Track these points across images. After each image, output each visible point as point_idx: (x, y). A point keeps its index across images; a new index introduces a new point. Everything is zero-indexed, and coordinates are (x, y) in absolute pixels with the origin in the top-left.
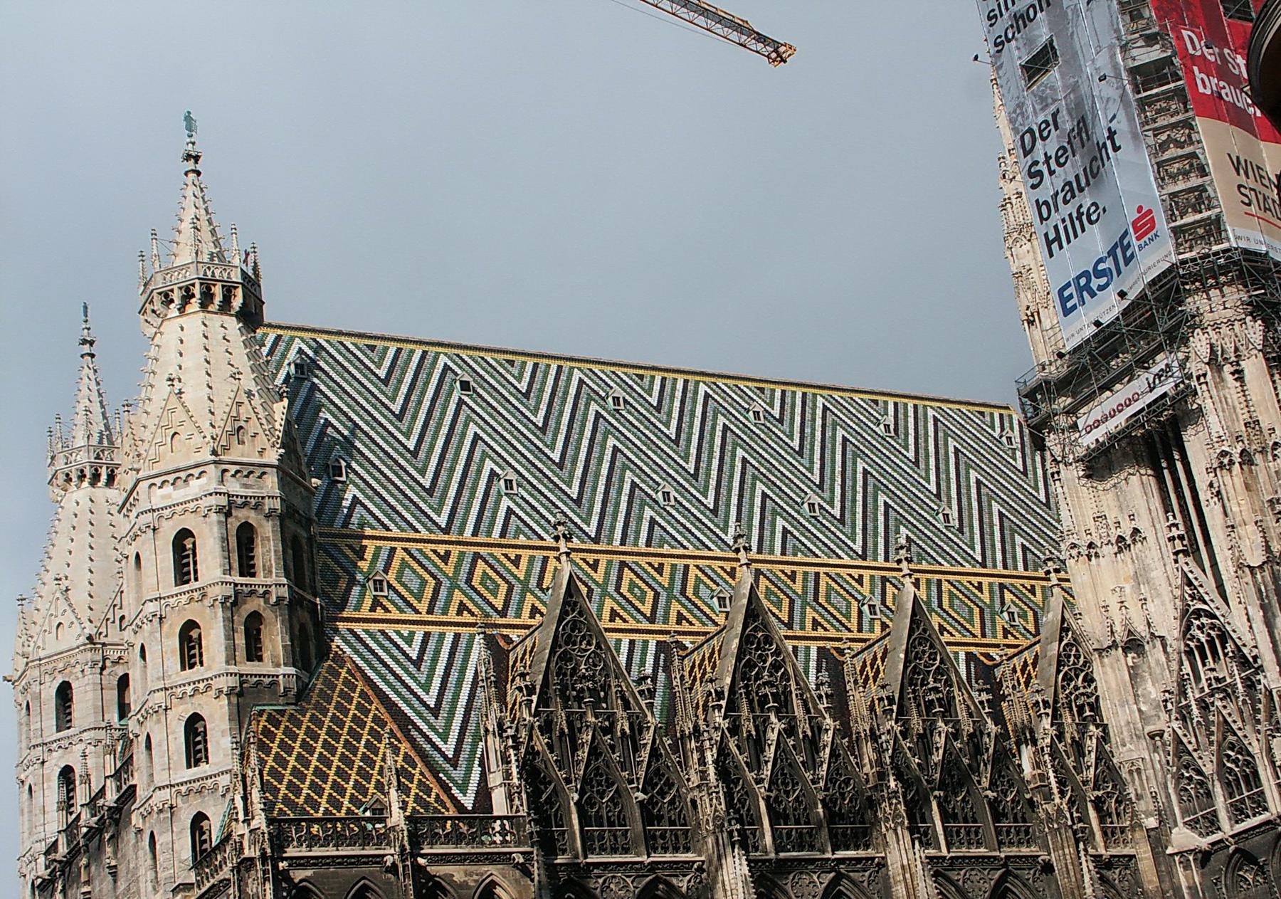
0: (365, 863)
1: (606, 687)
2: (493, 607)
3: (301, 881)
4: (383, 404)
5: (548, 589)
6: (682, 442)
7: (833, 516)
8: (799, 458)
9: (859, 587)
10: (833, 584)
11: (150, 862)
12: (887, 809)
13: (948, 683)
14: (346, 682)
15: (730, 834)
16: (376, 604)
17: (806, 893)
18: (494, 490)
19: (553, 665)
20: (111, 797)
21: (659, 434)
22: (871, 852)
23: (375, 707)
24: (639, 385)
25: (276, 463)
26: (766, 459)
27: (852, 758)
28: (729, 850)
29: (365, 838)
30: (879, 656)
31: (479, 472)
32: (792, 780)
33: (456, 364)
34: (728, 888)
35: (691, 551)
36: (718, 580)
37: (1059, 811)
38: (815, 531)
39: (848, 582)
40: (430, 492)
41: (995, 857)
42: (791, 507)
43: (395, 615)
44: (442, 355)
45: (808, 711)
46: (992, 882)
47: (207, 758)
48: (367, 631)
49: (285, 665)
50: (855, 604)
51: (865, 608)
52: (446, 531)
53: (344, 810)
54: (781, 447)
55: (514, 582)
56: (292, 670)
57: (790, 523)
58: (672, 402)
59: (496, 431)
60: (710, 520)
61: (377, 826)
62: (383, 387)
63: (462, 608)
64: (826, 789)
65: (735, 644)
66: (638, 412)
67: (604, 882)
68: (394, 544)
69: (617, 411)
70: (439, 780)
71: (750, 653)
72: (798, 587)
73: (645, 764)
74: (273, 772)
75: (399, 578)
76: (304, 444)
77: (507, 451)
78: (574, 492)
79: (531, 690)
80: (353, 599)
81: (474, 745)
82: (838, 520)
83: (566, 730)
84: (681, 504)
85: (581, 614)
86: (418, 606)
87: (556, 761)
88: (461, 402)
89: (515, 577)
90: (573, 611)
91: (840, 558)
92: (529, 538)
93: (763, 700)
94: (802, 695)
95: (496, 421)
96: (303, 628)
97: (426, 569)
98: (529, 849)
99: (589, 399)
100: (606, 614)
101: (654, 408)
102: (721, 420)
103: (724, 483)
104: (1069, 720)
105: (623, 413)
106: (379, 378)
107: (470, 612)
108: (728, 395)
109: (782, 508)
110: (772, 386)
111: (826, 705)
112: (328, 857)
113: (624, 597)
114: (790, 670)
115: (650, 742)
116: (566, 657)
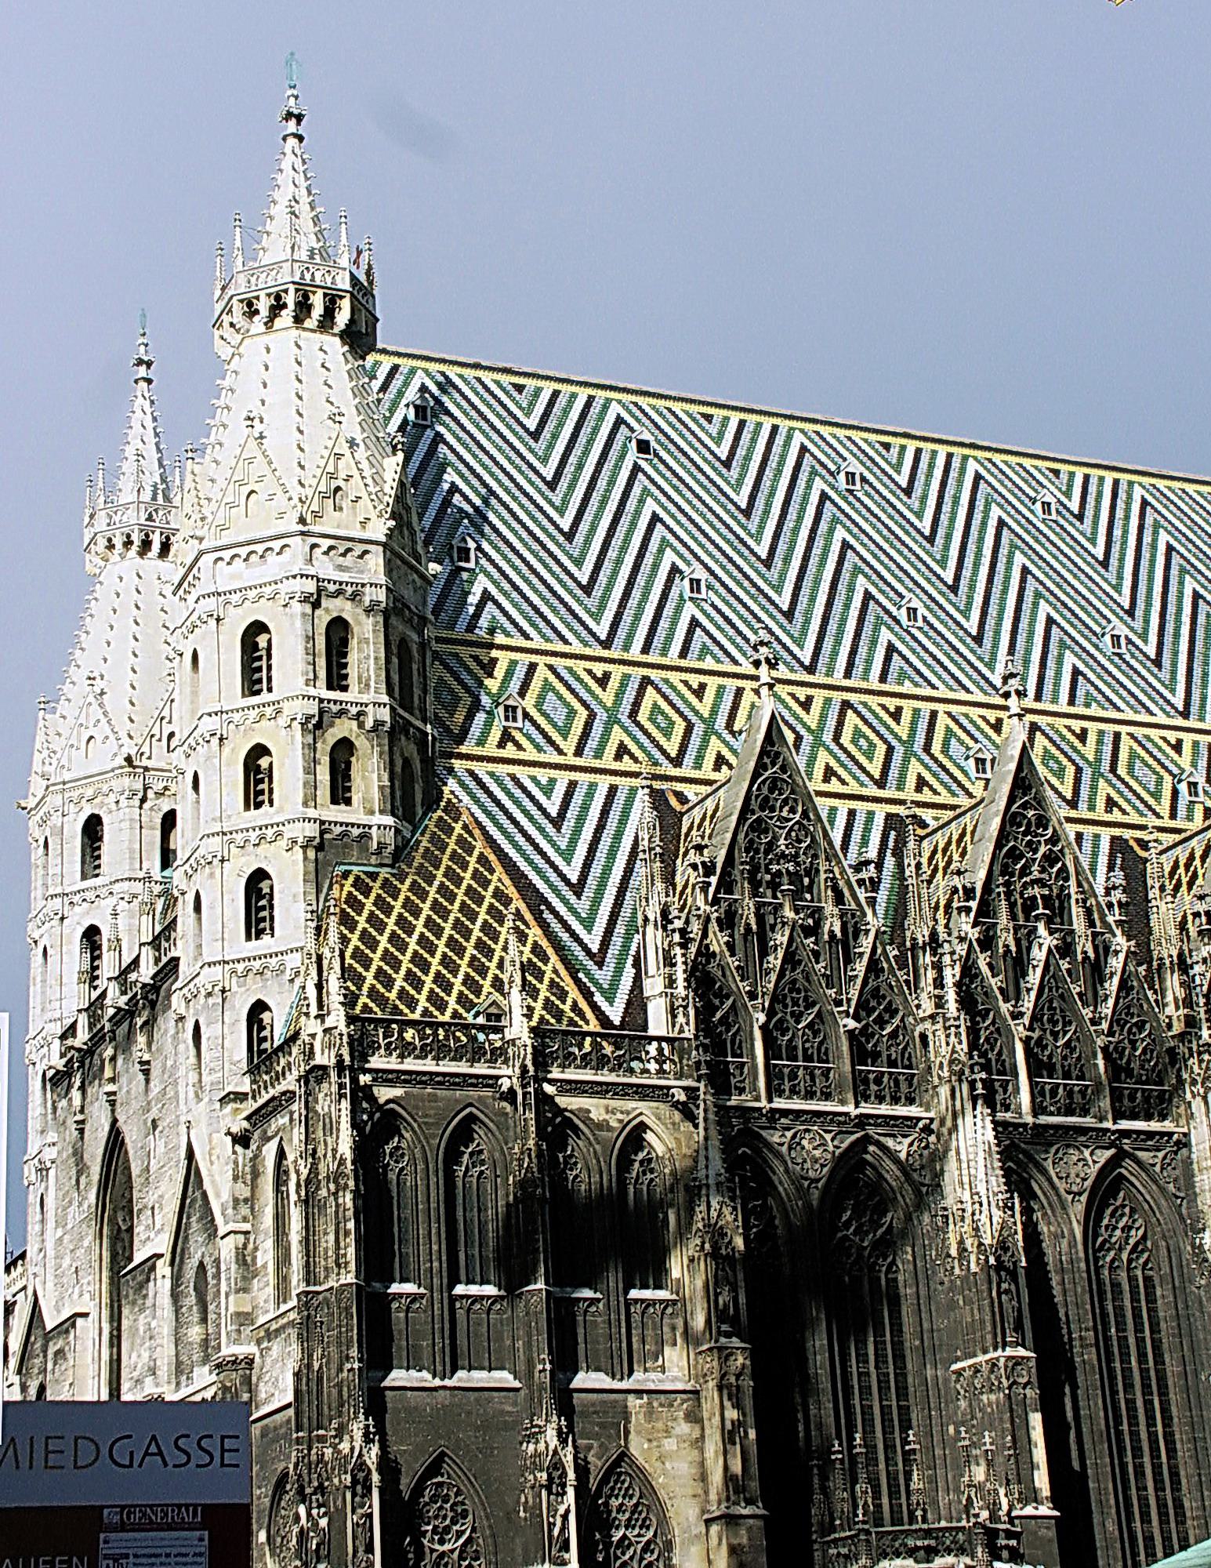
0: (472, 1085)
1: (812, 872)
2: (664, 752)
3: (389, 1101)
4: (530, 466)
5: (741, 732)
6: (939, 540)
7: (1145, 655)
8: (1103, 571)
9: (1175, 757)
10: (1139, 750)
11: (193, 1060)
12: (1196, 1069)
14: (460, 841)
15: (972, 1084)
16: (506, 738)
17: (1073, 1175)
18: (674, 593)
19: (741, 836)
20: (146, 972)
21: (907, 527)
22: (1167, 1125)
23: (499, 877)
24: (883, 457)
25: (383, 539)
26: (1055, 571)
27: (1149, 993)
28: (968, 1106)
29: (476, 1053)
30: (1198, 855)
31: (656, 567)
32: (1064, 1017)
33: (633, 416)
34: (963, 1157)
35: (943, 692)
36: (977, 734)
38: (1119, 675)
39: (1160, 749)
40: (588, 589)
42: (1086, 638)
43: (531, 754)
44: (614, 403)
45: (1091, 924)
47: (272, 929)
48: (492, 774)
49: (382, 812)
50: (1168, 778)
51: (1183, 788)
52: (606, 644)
53: (449, 1012)
54: (1078, 554)
55: (694, 719)
56: (389, 820)
57: (1084, 662)
58: (927, 484)
59: (682, 511)
60: (973, 651)
61: (491, 1036)
62: (531, 442)
63: (622, 751)
64: (1111, 1033)
65: (996, 823)
66: (880, 495)
67: (794, 1136)
68: (534, 658)
69: (851, 492)
70: (578, 982)
71: (1016, 839)
72: (1089, 751)
73: (859, 981)
74: (357, 954)
75: (538, 705)
76: (421, 516)
77: (696, 540)
78: (784, 602)
79: (709, 870)
80: (475, 730)
81: (628, 938)
82: (1153, 661)
83: (754, 927)
84: (931, 626)
85: (783, 769)
87: (738, 968)
88: (636, 469)
89: (696, 713)
90: (773, 764)
91: (1152, 714)
93: (1030, 905)
94: (1084, 901)
95: (683, 496)
98: (695, 1084)
99: (814, 473)
100: (819, 772)
101: (903, 490)
102: (996, 512)
105: (859, 495)
106: (527, 430)
107: (633, 757)
108: (1007, 477)
109: (1073, 639)
110: (1072, 468)
111: (1118, 918)
112: (424, 1073)
113: (845, 750)
115: (869, 951)
116: (759, 827)
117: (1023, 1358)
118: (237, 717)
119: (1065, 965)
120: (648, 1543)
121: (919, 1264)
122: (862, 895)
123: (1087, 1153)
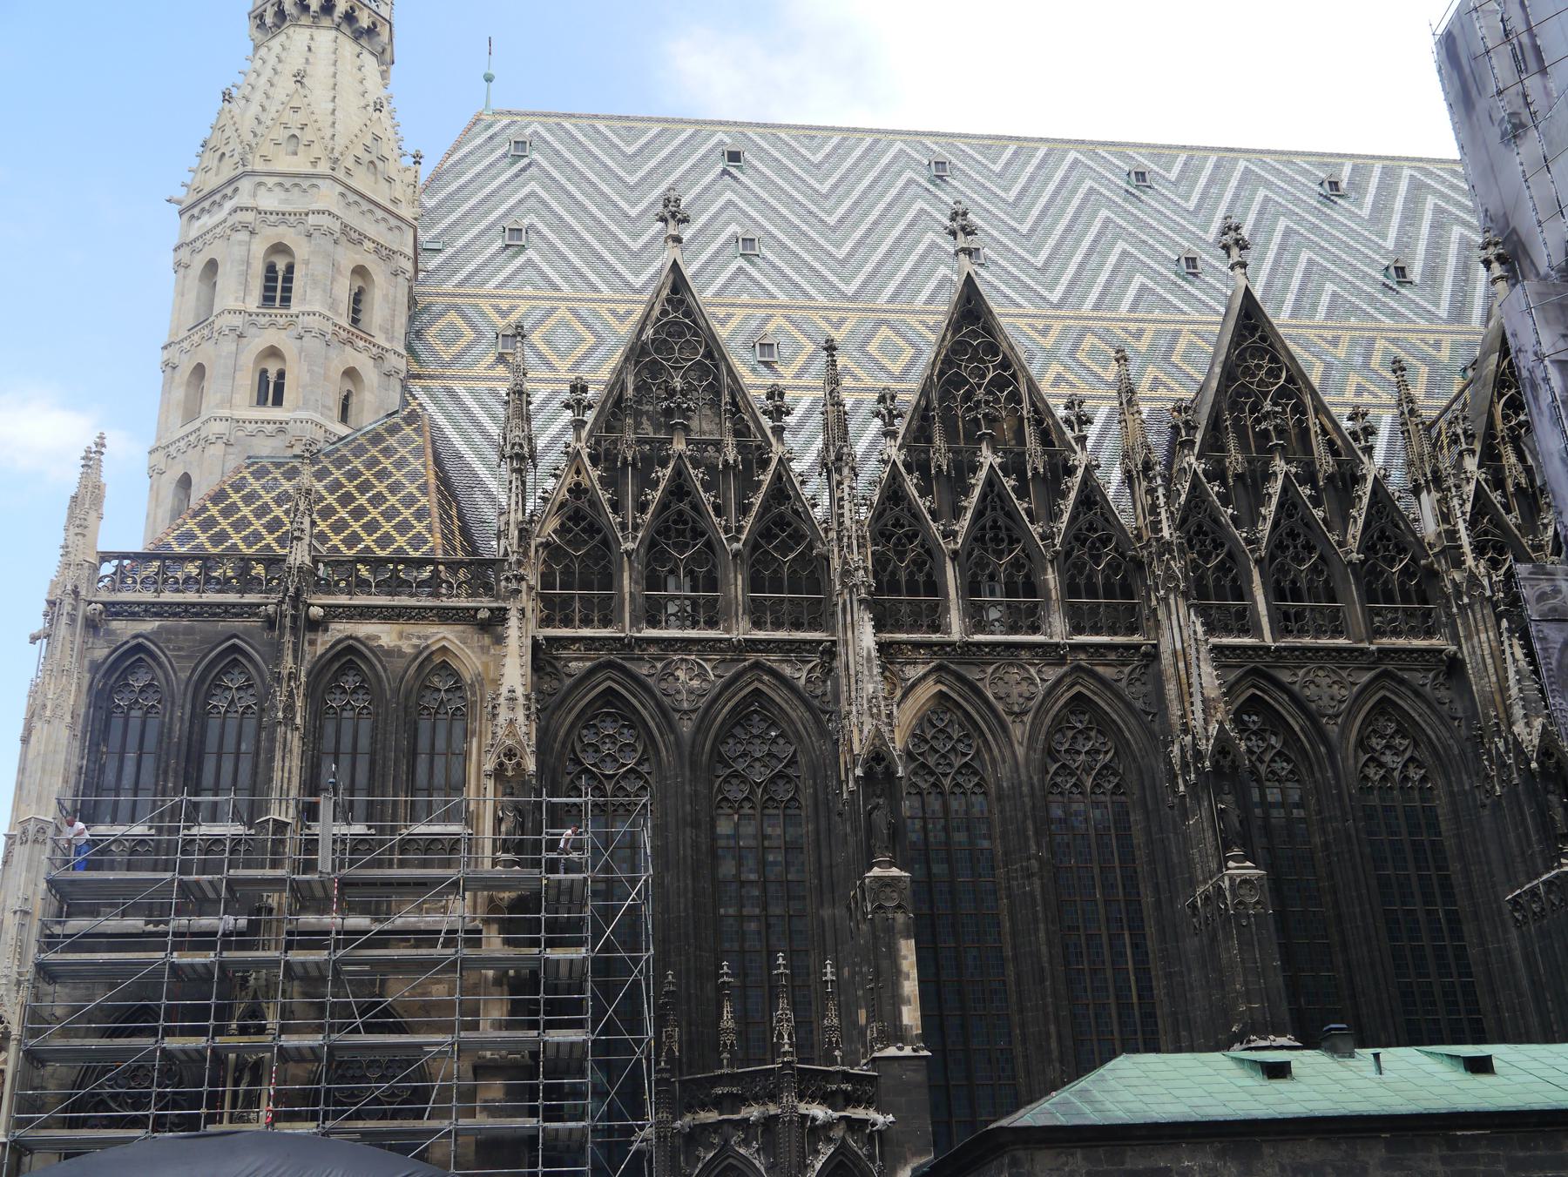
0: (236, 615)
3: (136, 636)
13: (1299, 409)
32: (1010, 537)
34: (852, 672)
37: (1473, 579)
41: (1363, 651)
46: (1355, 689)
67: (664, 668)
68: (555, 304)
71: (959, 366)
73: (755, 509)
80: (468, 359)
87: (609, 500)
92: (752, 296)
96: (351, 373)
104: (1513, 460)
114: (1023, 389)
117: (893, 878)
118: (186, 345)
119: (1009, 483)
121: (821, 796)
122: (767, 423)
123: (1033, 671)
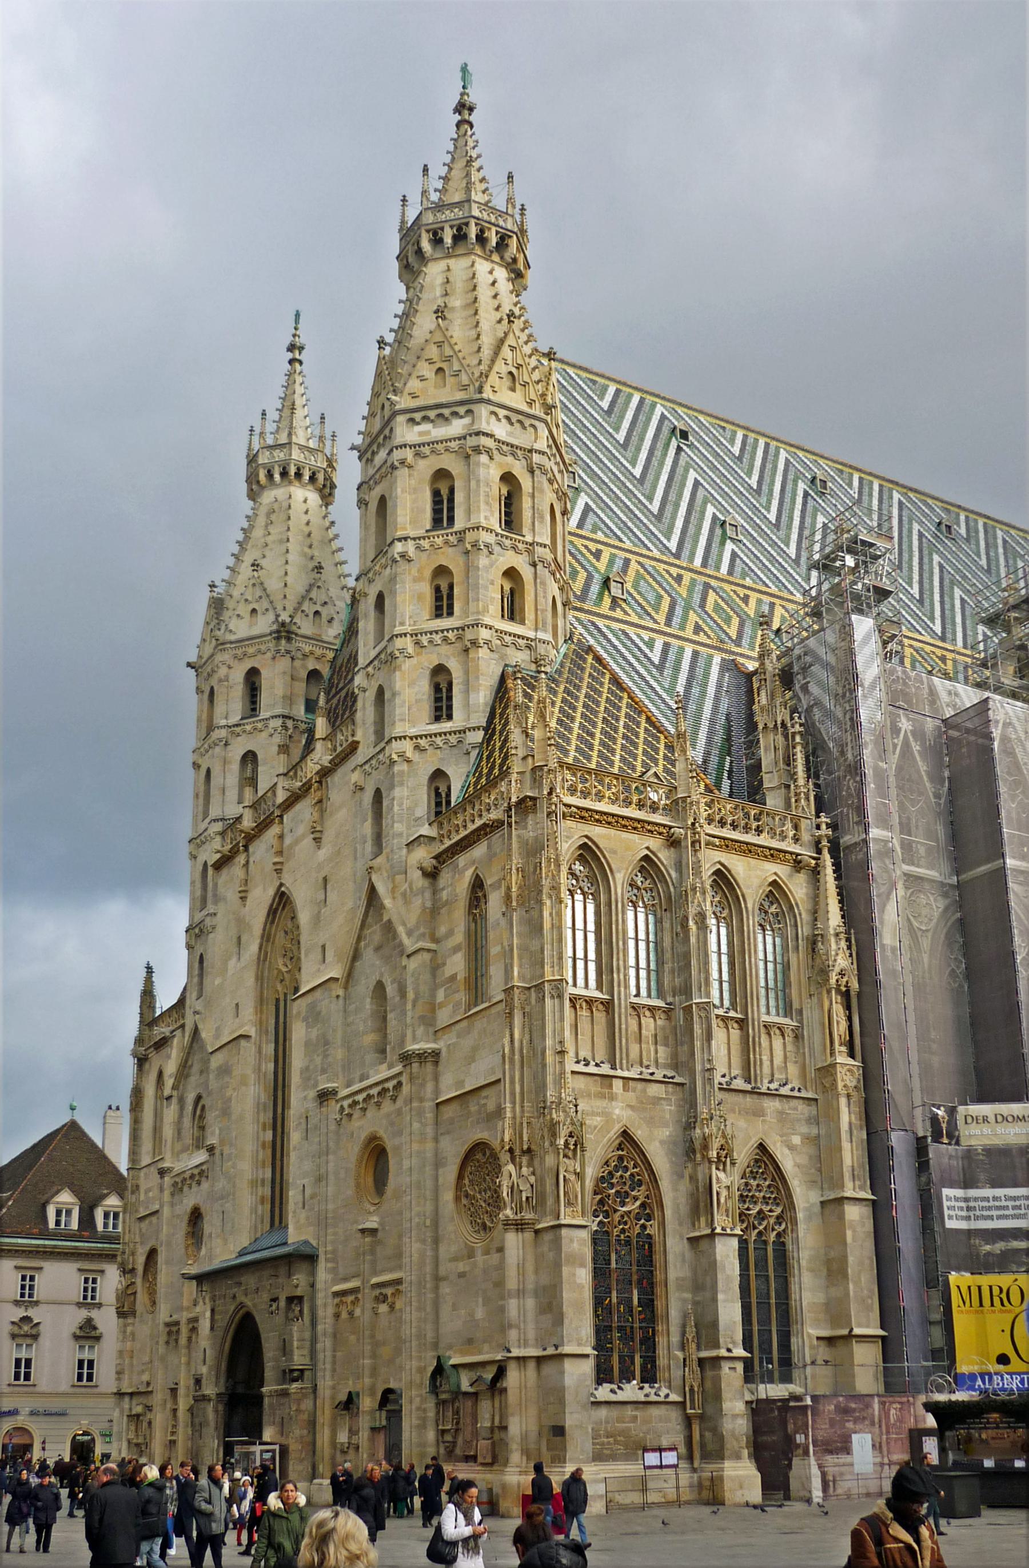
2: (727, 634)
5: (779, 630)
20: (321, 755)
43: (634, 619)
48: (608, 627)
52: (677, 555)
63: (698, 629)
75: (635, 586)
86: (656, 616)
88: (679, 449)
92: (754, 582)
97: (661, 585)
102: (916, 527)
103: (926, 581)
107: (705, 633)
112: (613, 815)
120: (778, 1218)
